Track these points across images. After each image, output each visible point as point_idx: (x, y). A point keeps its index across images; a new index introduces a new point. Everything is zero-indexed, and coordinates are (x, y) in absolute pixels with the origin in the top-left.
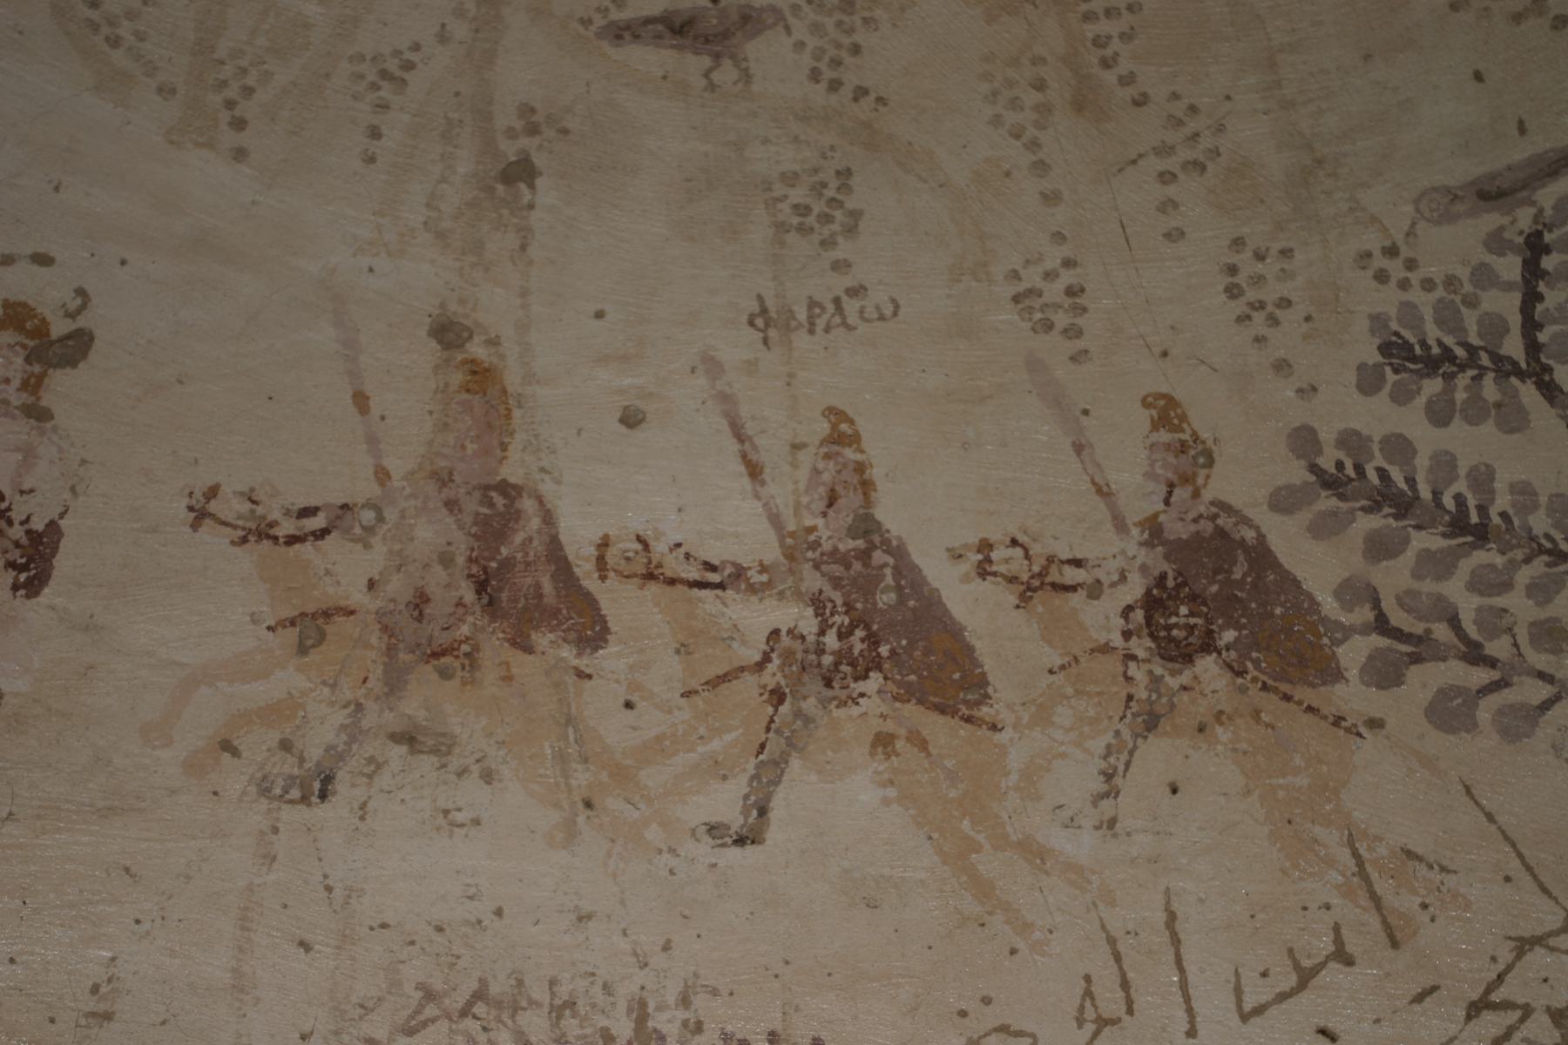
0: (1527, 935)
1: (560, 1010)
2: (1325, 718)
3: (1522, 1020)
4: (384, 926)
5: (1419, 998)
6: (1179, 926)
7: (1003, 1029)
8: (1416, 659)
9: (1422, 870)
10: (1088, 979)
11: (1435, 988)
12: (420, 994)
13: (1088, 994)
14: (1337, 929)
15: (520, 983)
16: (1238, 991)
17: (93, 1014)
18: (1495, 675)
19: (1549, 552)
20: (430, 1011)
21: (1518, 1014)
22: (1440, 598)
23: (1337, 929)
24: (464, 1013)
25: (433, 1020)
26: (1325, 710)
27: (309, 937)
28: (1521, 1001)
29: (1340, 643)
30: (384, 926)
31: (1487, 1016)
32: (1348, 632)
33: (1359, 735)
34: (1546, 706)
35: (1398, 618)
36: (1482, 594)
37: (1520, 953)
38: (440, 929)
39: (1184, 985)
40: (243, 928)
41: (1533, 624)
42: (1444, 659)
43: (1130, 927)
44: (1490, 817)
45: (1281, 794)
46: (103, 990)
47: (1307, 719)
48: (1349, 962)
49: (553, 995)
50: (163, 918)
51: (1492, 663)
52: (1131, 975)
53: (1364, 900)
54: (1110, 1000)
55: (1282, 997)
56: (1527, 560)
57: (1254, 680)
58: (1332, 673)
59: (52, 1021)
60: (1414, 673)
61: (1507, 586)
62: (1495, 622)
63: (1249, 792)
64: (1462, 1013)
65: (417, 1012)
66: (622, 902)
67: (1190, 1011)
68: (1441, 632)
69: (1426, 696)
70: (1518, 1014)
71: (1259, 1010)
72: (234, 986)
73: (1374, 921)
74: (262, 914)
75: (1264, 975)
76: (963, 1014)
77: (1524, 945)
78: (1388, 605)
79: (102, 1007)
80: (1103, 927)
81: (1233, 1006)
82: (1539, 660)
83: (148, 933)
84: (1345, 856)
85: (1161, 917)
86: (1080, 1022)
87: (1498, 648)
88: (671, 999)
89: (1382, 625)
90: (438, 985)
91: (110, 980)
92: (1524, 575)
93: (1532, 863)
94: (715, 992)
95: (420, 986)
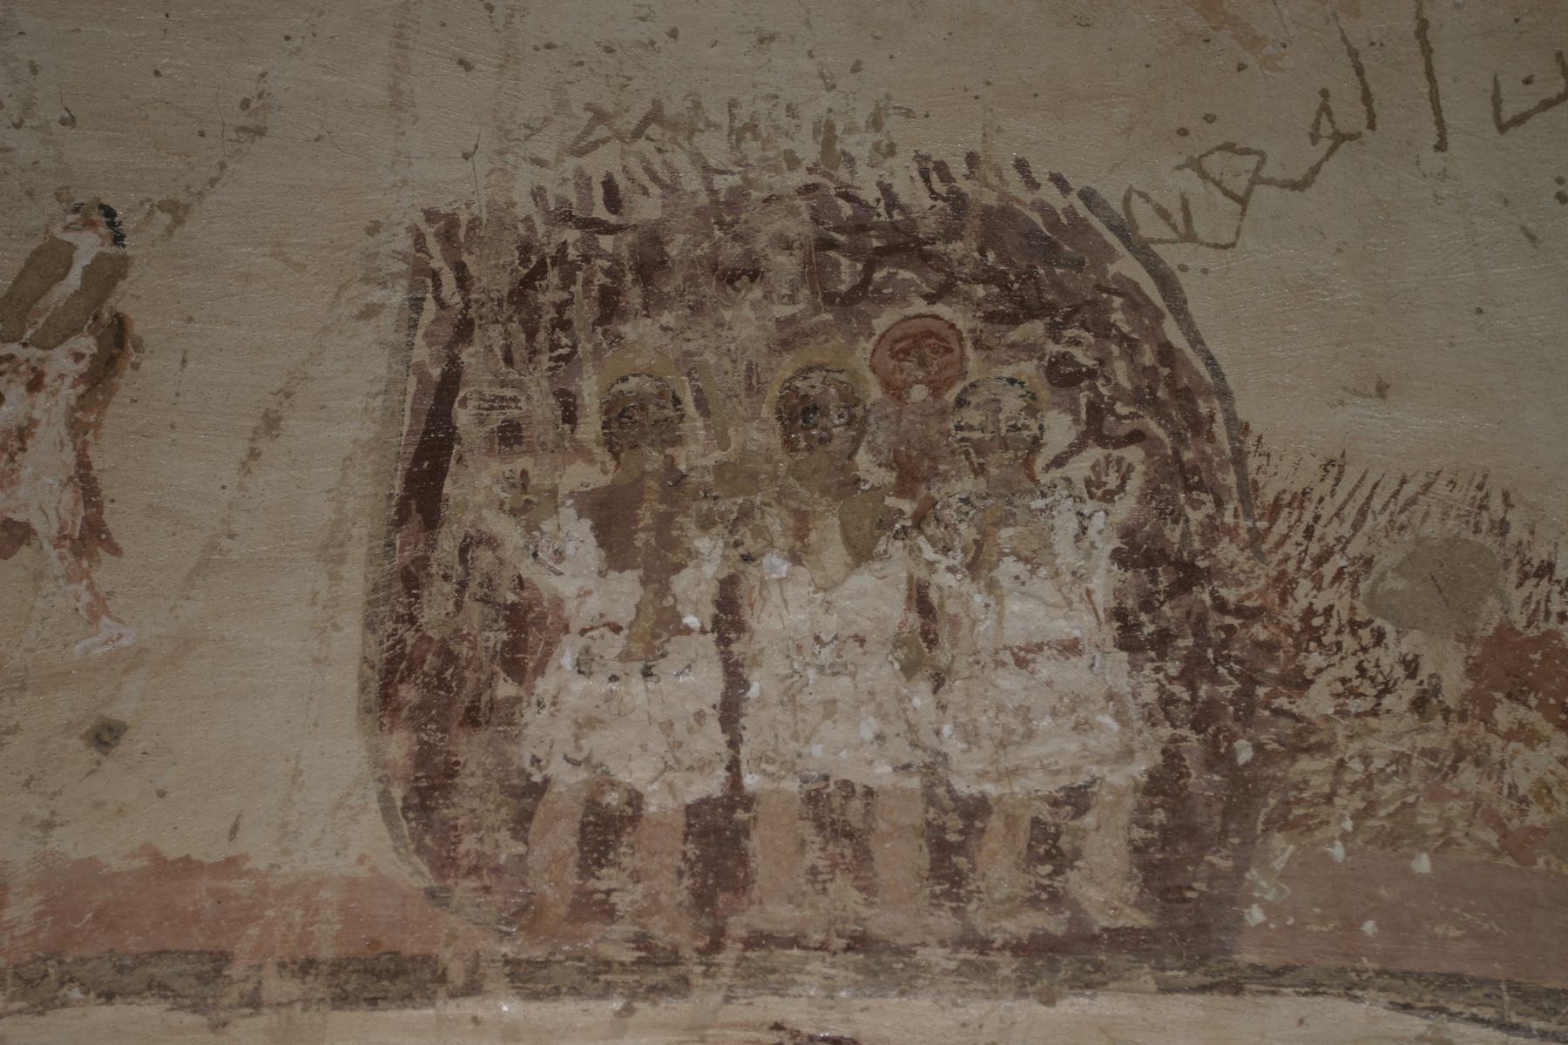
1: (741, 132)
4: (550, 46)
6: (1430, 34)
7: (1228, 147)
10: (1325, 94)
12: (590, 115)
13: (1325, 109)
15: (697, 105)
16: (1497, 101)
17: (244, 129)
20: (601, 131)
24: (637, 134)
25: (604, 141)
27: (469, 56)
30: (550, 46)
38: (609, 50)
39: (1434, 97)
40: (398, 46)
43: (1375, 38)
46: (253, 105)
49: (732, 117)
50: (314, 35)
52: (1373, 88)
54: (1349, 114)
55: (1547, 105)
59: (202, 134)
65: (587, 133)
66: (808, 23)
67: (1440, 123)
71: (1519, 120)
72: (391, 104)
74: (418, 32)
75: (1527, 82)
76: (1183, 132)
79: (251, 122)
80: (1344, 39)
81: (1489, 116)
83: (298, 49)
85: (1410, 26)
86: (1315, 138)
88: (861, 123)
90: (608, 107)
91: (260, 96)
94: (908, 114)
95: (589, 107)
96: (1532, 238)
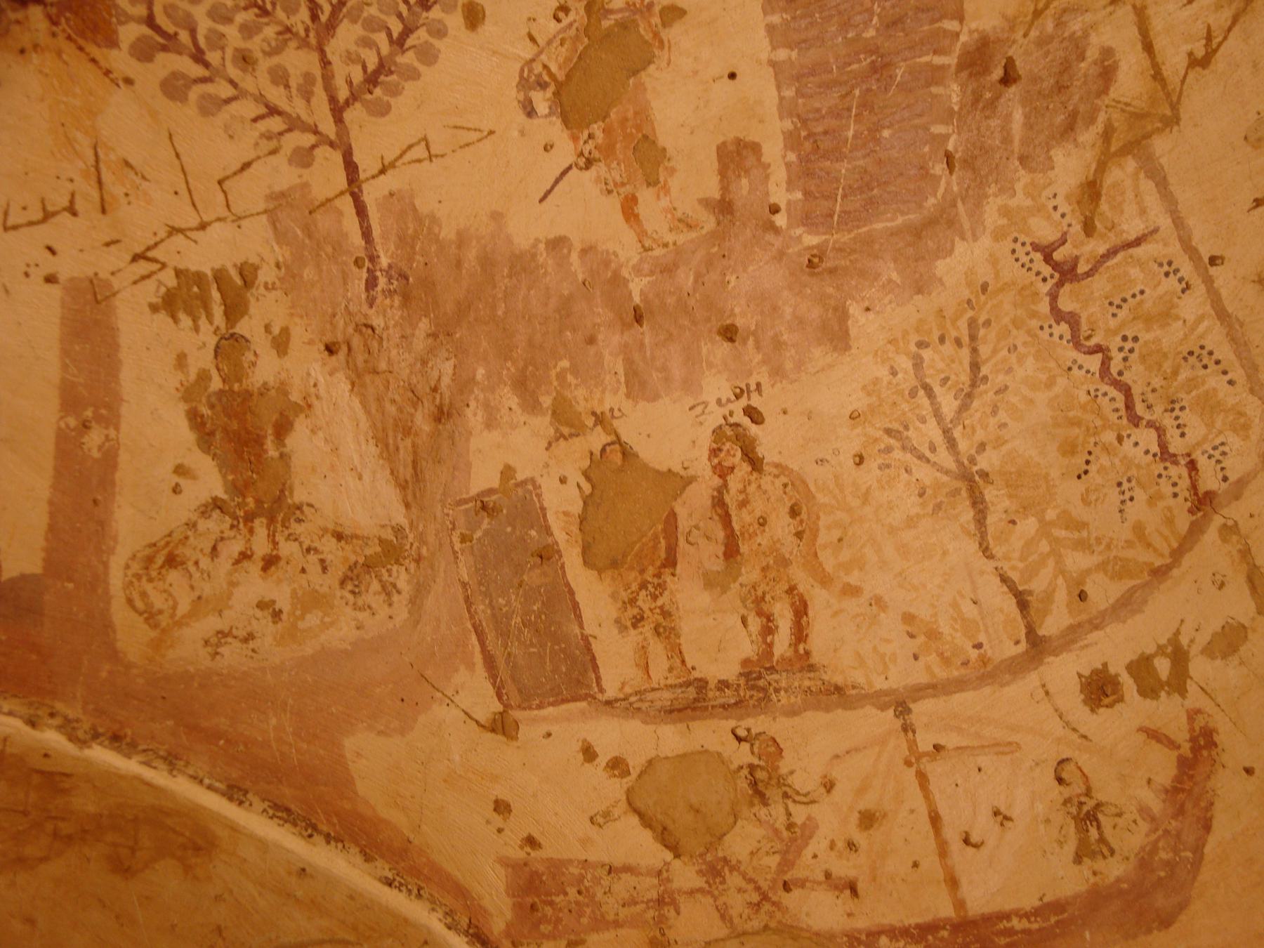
0: (176, 226)
2: (100, 68)
3: (160, 270)
5: (108, 244)
8: (164, 48)
9: (132, 175)
11: (117, 241)
14: (73, 195)
18: (206, 73)
19: (259, 8)
21: (159, 266)
22: (189, 15)
23: (73, 195)
26: (103, 63)
28: (162, 259)
29: (121, 23)
31: (142, 263)
32: (129, 18)
33: (118, 85)
34: (228, 101)
35: (161, 20)
36: (214, 21)
37: (170, 234)
41: (236, 50)
42: (180, 53)
44: (178, 156)
45: (62, 106)
47: (90, 66)
48: (75, 214)
51: (207, 65)
53: (93, 181)
55: (31, 224)
56: (246, 9)
57: (64, 31)
58: (113, 43)
60: (161, 57)
61: (228, 20)
62: (218, 41)
63: (42, 100)
64: (129, 258)
68: (184, 36)
69: (163, 74)
70: (159, 266)
71: (15, 228)
73: (95, 195)
75: (24, 208)
77: (174, 231)
78: (158, 9)
82: (233, 72)
84: (90, 154)
87: (213, 57)
89: (150, 21)
92: (241, 17)
93: (192, 189)
96: (7, 291)
